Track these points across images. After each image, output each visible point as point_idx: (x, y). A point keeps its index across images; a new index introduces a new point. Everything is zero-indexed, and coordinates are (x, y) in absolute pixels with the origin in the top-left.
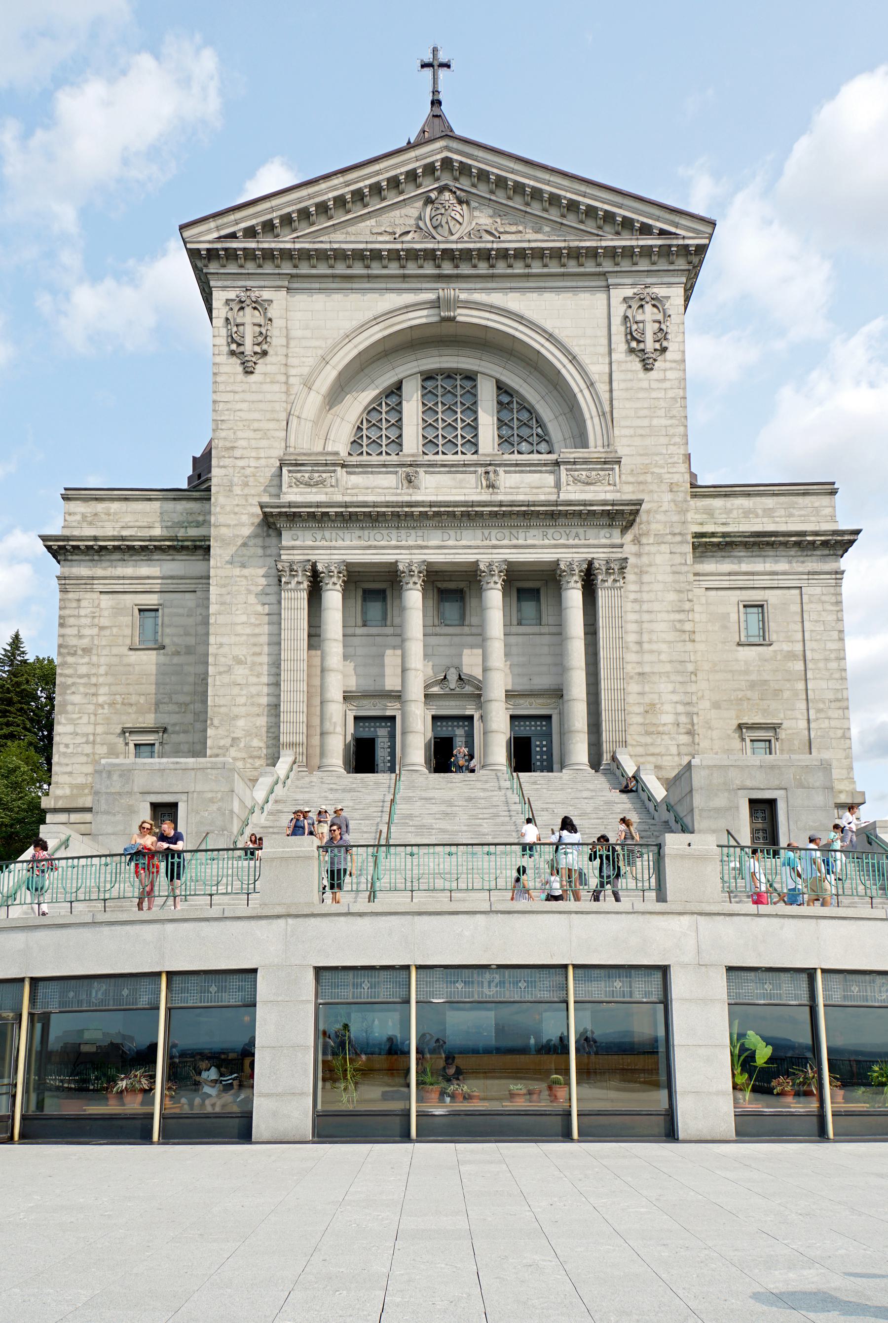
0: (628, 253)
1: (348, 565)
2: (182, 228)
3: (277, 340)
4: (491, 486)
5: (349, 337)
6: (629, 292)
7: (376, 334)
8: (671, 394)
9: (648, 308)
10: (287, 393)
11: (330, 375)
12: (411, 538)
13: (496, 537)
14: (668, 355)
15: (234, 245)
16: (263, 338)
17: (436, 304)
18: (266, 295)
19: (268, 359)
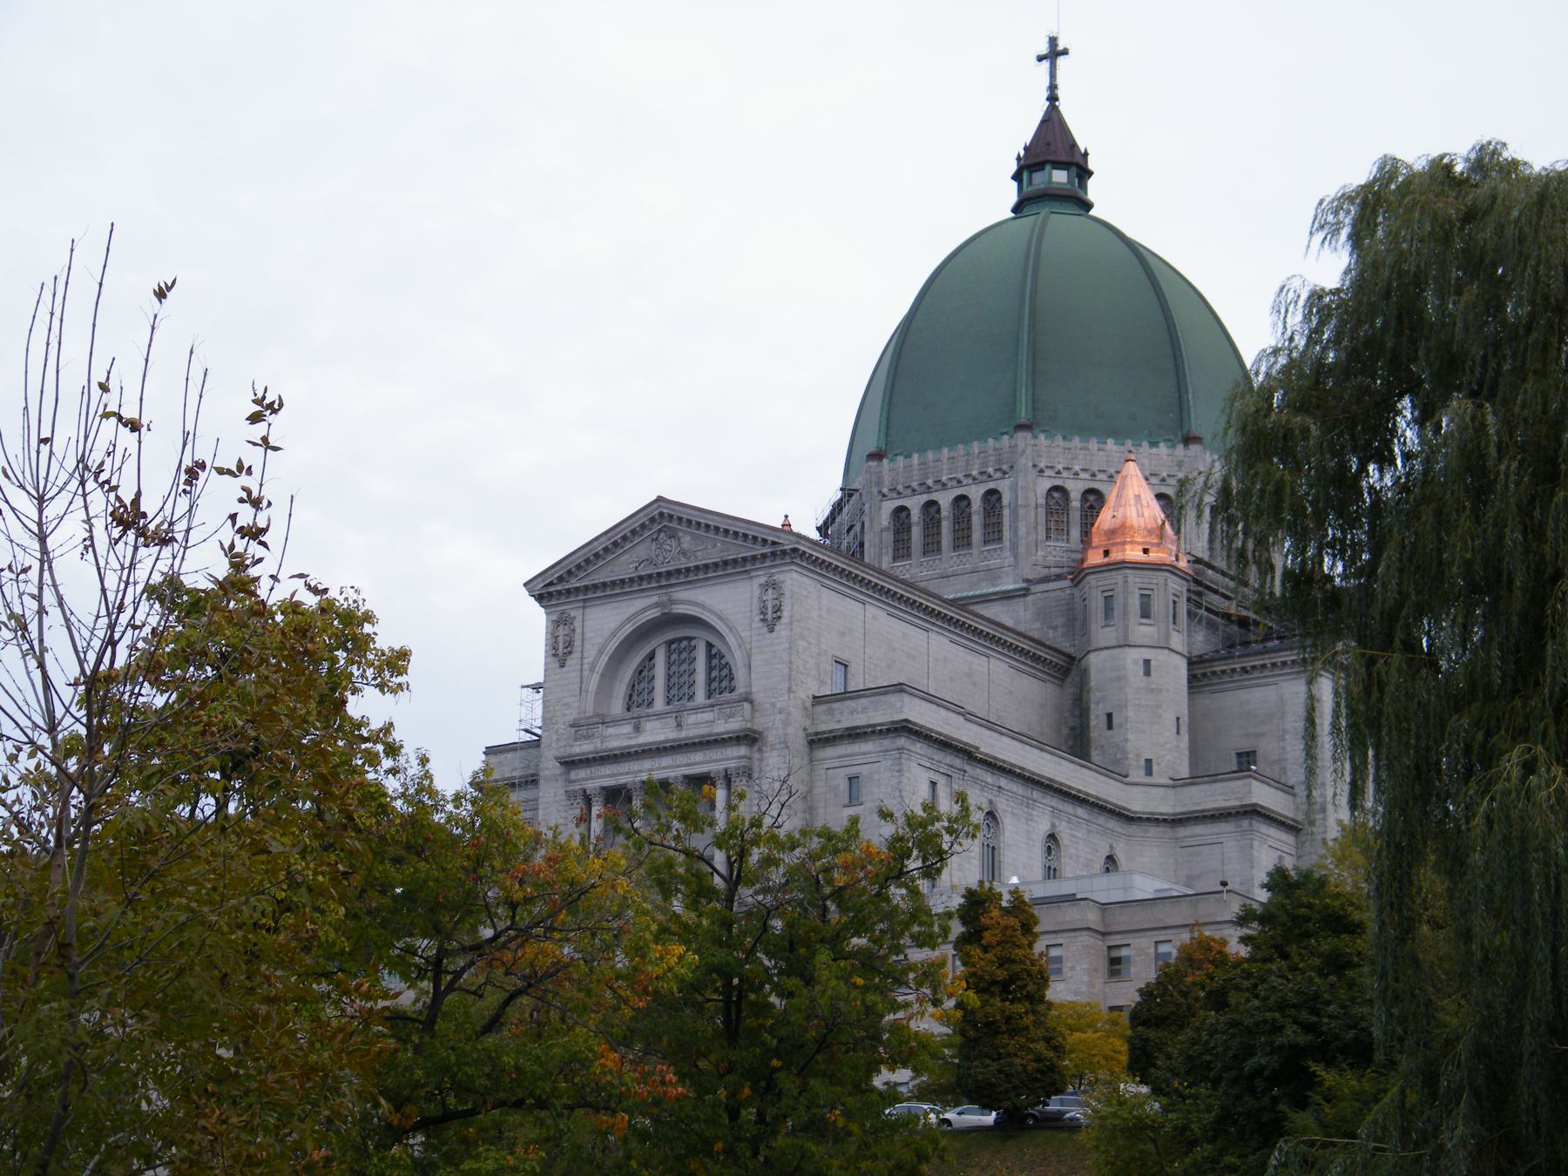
0: (754, 558)
1: (603, 788)
2: (525, 585)
3: (578, 643)
4: (679, 725)
5: (614, 635)
6: (763, 580)
7: (629, 629)
8: (783, 646)
9: (770, 590)
10: (581, 677)
11: (605, 659)
12: (634, 766)
13: (681, 759)
14: (785, 620)
15: (552, 589)
16: (569, 644)
17: (656, 605)
18: (573, 614)
19: (573, 656)
